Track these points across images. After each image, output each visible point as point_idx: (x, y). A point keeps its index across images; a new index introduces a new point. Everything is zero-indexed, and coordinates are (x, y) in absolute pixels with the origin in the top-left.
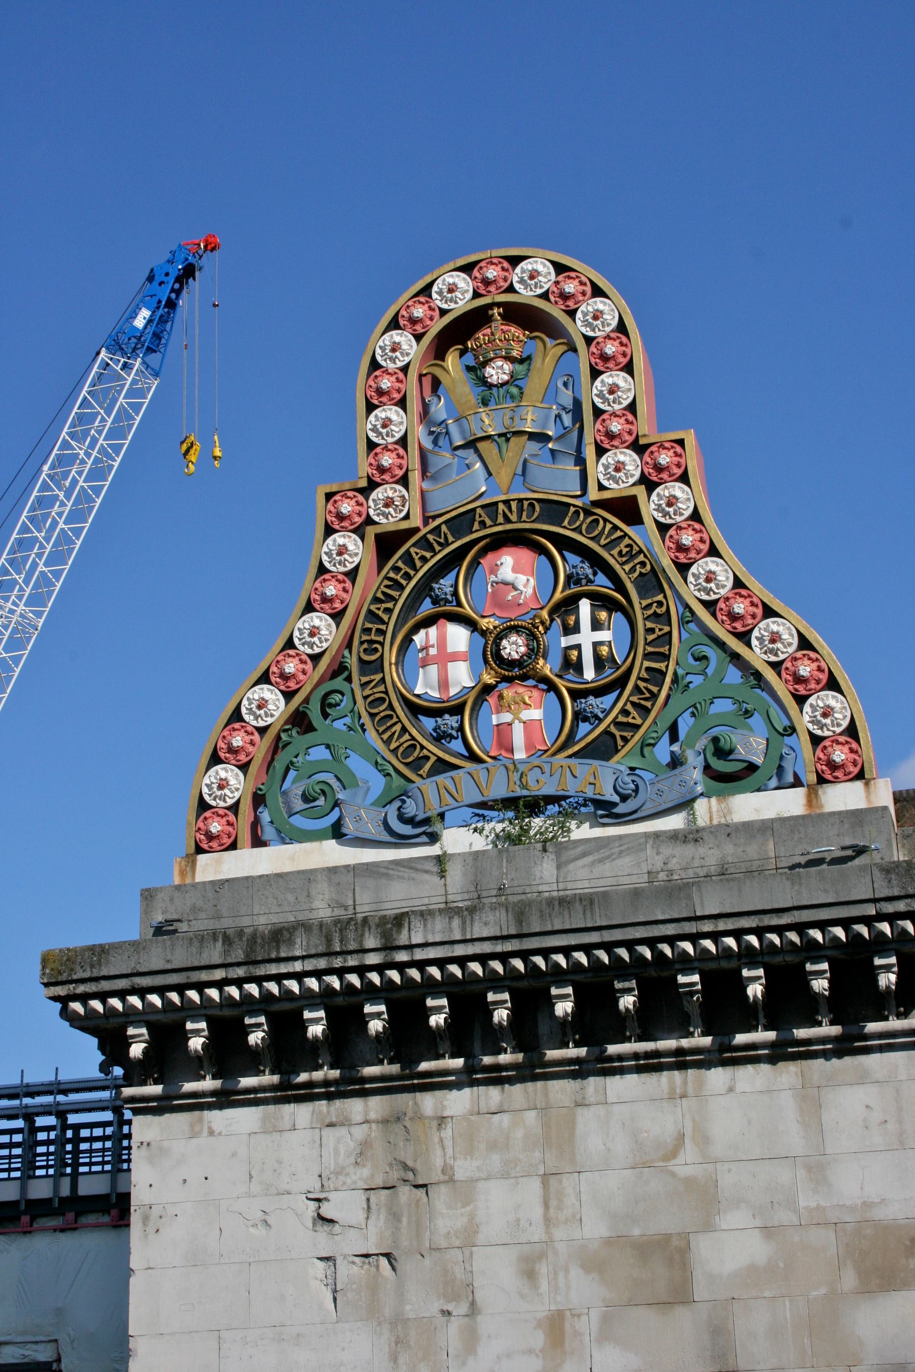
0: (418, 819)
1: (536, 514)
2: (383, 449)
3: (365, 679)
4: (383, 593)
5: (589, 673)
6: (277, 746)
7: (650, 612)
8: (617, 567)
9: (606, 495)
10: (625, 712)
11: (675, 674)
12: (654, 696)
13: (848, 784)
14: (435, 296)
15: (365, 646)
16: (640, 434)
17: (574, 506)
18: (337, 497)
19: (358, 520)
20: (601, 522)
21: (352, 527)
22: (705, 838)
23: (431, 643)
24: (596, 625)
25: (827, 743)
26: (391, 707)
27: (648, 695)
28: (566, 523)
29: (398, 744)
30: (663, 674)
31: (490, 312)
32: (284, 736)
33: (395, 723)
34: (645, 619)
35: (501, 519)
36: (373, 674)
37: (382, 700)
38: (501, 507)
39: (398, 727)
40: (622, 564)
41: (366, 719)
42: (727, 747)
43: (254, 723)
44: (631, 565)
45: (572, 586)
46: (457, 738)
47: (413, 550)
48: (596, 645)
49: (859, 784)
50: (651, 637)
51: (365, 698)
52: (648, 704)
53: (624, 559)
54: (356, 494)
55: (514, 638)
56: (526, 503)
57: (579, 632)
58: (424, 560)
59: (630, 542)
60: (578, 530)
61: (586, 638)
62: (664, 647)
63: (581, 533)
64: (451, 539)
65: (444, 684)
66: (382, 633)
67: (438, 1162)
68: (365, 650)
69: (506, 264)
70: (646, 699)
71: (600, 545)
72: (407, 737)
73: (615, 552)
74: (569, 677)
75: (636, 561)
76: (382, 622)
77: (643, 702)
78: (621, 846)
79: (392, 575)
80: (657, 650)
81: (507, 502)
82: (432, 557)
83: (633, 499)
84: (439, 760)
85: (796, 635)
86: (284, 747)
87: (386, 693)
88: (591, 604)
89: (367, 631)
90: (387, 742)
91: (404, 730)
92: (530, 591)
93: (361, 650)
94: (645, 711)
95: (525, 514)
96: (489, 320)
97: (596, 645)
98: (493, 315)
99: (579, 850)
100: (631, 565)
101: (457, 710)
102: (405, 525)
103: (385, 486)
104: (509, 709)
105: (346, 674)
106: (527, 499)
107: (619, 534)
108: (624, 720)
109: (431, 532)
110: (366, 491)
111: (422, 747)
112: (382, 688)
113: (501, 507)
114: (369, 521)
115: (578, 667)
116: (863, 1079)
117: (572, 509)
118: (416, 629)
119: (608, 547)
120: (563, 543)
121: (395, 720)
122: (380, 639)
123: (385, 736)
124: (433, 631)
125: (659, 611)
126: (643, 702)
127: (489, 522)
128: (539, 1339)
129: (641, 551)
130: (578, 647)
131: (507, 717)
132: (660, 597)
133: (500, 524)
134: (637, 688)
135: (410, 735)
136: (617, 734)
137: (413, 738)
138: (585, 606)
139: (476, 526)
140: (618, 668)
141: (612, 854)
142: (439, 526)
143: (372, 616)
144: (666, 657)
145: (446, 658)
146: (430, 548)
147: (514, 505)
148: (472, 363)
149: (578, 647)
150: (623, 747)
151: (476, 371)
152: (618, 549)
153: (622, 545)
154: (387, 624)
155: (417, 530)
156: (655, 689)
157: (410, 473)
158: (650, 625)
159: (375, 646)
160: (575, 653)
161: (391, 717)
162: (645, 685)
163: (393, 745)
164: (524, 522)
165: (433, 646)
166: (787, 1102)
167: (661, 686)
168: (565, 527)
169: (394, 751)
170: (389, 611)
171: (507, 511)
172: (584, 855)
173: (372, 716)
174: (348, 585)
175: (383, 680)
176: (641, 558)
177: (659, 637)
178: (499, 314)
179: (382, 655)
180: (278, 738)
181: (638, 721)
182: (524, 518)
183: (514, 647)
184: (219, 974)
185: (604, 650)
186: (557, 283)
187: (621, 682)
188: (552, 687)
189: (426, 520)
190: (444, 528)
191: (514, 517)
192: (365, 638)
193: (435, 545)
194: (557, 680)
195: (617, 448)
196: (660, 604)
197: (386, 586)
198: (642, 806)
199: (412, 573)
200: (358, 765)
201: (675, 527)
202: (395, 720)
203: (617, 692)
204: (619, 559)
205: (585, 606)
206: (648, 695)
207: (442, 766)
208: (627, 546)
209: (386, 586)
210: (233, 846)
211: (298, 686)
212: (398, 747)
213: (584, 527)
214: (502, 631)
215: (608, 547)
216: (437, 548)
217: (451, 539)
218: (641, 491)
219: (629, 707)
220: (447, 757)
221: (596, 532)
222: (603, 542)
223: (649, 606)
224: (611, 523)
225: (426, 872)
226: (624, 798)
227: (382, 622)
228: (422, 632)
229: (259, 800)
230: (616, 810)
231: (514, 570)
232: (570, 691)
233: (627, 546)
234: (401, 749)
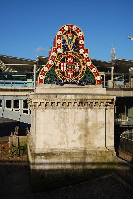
5: (77, 71)
24: (78, 66)
67: (65, 116)
84: (64, 78)
115: (76, 70)
116: (101, 111)
118: (61, 63)
119: (80, 59)
124: (63, 64)
128: (73, 131)
130: (76, 68)
138: (77, 64)
143: (57, 61)
145: (64, 67)
149: (76, 68)
166: (95, 113)
184: (48, 99)
205: (77, 64)
210: (43, 83)
215: (80, 59)
229: (45, 79)
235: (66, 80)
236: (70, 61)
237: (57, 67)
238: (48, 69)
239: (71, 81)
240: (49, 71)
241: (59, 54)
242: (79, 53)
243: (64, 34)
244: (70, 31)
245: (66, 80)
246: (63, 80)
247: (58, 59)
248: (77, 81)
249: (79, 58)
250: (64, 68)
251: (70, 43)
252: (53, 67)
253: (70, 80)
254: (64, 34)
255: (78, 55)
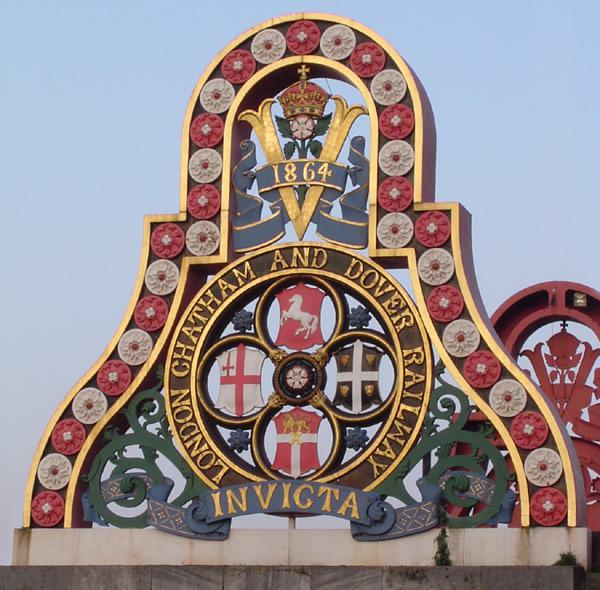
0: (208, 521)
1: (324, 263)
2: (201, 188)
3: (174, 393)
4: (193, 317)
6: (99, 443)
7: (411, 362)
8: (387, 319)
9: (383, 253)
10: (381, 446)
11: (426, 417)
12: (407, 436)
13: (554, 529)
14: (253, 50)
15: (176, 363)
16: (415, 201)
17: (356, 258)
18: (160, 228)
19: (177, 250)
20: (377, 274)
21: (171, 256)
22: (429, 577)
23: (231, 365)
25: (540, 492)
26: (194, 419)
27: (402, 434)
28: (348, 273)
29: (198, 452)
30: (416, 417)
31: (299, 71)
32: (107, 435)
33: (197, 434)
34: (405, 367)
35: (294, 264)
36: (182, 388)
37: (186, 413)
38: (296, 251)
39: (198, 438)
40: (390, 317)
41: (172, 427)
42: (460, 487)
43: (81, 421)
44: (398, 318)
45: (350, 328)
46: (247, 449)
47: (220, 282)
48: (364, 383)
49: (562, 530)
50: (408, 384)
51: (173, 409)
52: (402, 442)
53: (394, 311)
54: (176, 226)
55: (297, 370)
56: (316, 251)
57: (351, 370)
58: (229, 292)
59: (399, 297)
60: (356, 281)
61: (357, 376)
62: (418, 393)
63: (359, 284)
64: (253, 276)
65: (240, 403)
66: (190, 353)
68: (176, 367)
69: (315, 27)
70: (400, 437)
71: (375, 298)
72: (205, 447)
73: (386, 305)
74: (341, 408)
75: (403, 314)
76: (192, 344)
77: (398, 440)
78: (364, 576)
79: (202, 302)
80: (412, 395)
81: (301, 248)
82: (236, 290)
83: (406, 258)
85: (526, 396)
86: (109, 442)
87: (191, 406)
88: (364, 346)
89: (177, 350)
90: (189, 451)
91: (203, 441)
92: (314, 328)
93: (174, 365)
94: (397, 448)
95: (315, 260)
96: (297, 77)
97: (364, 383)
98: (301, 74)
99: (328, 576)
100: (398, 318)
101: (250, 425)
102: (214, 260)
103: (201, 222)
104: (289, 431)
105: (160, 384)
106: (318, 248)
107: (390, 288)
108: (381, 453)
109: (236, 267)
110: (185, 225)
111: (217, 458)
112: (187, 402)
113: (296, 251)
114: (184, 252)
115: (348, 402)
117: (354, 261)
119: (379, 299)
120: (342, 289)
121: (197, 431)
122: (189, 358)
123: (188, 445)
124: (234, 351)
125: (417, 361)
126: (398, 440)
127: (285, 265)
129: (407, 306)
130: (349, 384)
131: (286, 438)
132: (419, 350)
133: (294, 267)
134: (393, 428)
135: (208, 445)
136: (375, 464)
137: (210, 449)
138: (358, 346)
139: (274, 267)
140: (383, 405)
141: (355, 583)
142: (244, 263)
143: (182, 337)
144: (419, 403)
145: (239, 380)
146: (234, 281)
147: (306, 252)
148: (282, 116)
149: (349, 384)
150: (378, 476)
151: (283, 124)
152: (388, 302)
153: (393, 298)
154: (196, 346)
155: (221, 266)
156: (408, 429)
157: (222, 213)
158: (408, 373)
159: (185, 364)
160: (345, 389)
161: (193, 428)
162: (401, 425)
163: (194, 454)
164: (314, 268)
165: (233, 368)
167: (412, 426)
168: (346, 277)
169: (194, 459)
170: (197, 334)
171: (300, 255)
172: (334, 580)
173: (179, 427)
174: (165, 306)
175: (189, 396)
176: (407, 313)
177: (416, 384)
178: (307, 73)
179: (189, 374)
180: (101, 434)
181: (393, 456)
182: (314, 264)
183: (297, 378)
185: (369, 389)
186: (356, 51)
187: (383, 417)
188: (326, 415)
189: (233, 255)
190: (247, 264)
191: (305, 263)
192: (176, 356)
193: (240, 280)
194: (331, 413)
195: (395, 211)
196: (418, 355)
197: (197, 312)
198: (387, 532)
199: (219, 302)
200: (163, 463)
201: (436, 289)
202: (197, 431)
203: (380, 424)
204: (389, 311)
205: (358, 347)
206: (402, 434)
207: (231, 480)
208: (396, 300)
209: (197, 312)
210: (60, 525)
211: (120, 392)
212: (198, 455)
213: (363, 278)
214: (290, 361)
216: (241, 283)
217: (253, 276)
218: (410, 253)
219: (386, 442)
220: (237, 468)
221: (372, 285)
222: (378, 293)
223: (409, 357)
224: (385, 277)
225: (209, 579)
226: (375, 522)
227: (192, 344)
228: (225, 355)
229: (82, 486)
230: (371, 531)
231: (304, 308)
232: (338, 420)
233: (396, 300)
234: (200, 457)
235: (243, 491)
236: (298, 323)
237: (180, 383)
238: (111, 400)
239: (286, 504)
240: (119, 422)
241: (198, 274)
242: (372, 242)
243: (252, 101)
244: (303, 71)
245: (243, 491)
246: (216, 497)
247: (187, 323)
248: (343, 497)
249: (371, 291)
250: (246, 386)
251: (300, 166)
252: (153, 380)
253: (279, 493)
254: (252, 101)
255: (367, 266)
